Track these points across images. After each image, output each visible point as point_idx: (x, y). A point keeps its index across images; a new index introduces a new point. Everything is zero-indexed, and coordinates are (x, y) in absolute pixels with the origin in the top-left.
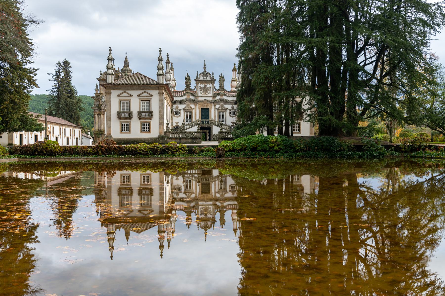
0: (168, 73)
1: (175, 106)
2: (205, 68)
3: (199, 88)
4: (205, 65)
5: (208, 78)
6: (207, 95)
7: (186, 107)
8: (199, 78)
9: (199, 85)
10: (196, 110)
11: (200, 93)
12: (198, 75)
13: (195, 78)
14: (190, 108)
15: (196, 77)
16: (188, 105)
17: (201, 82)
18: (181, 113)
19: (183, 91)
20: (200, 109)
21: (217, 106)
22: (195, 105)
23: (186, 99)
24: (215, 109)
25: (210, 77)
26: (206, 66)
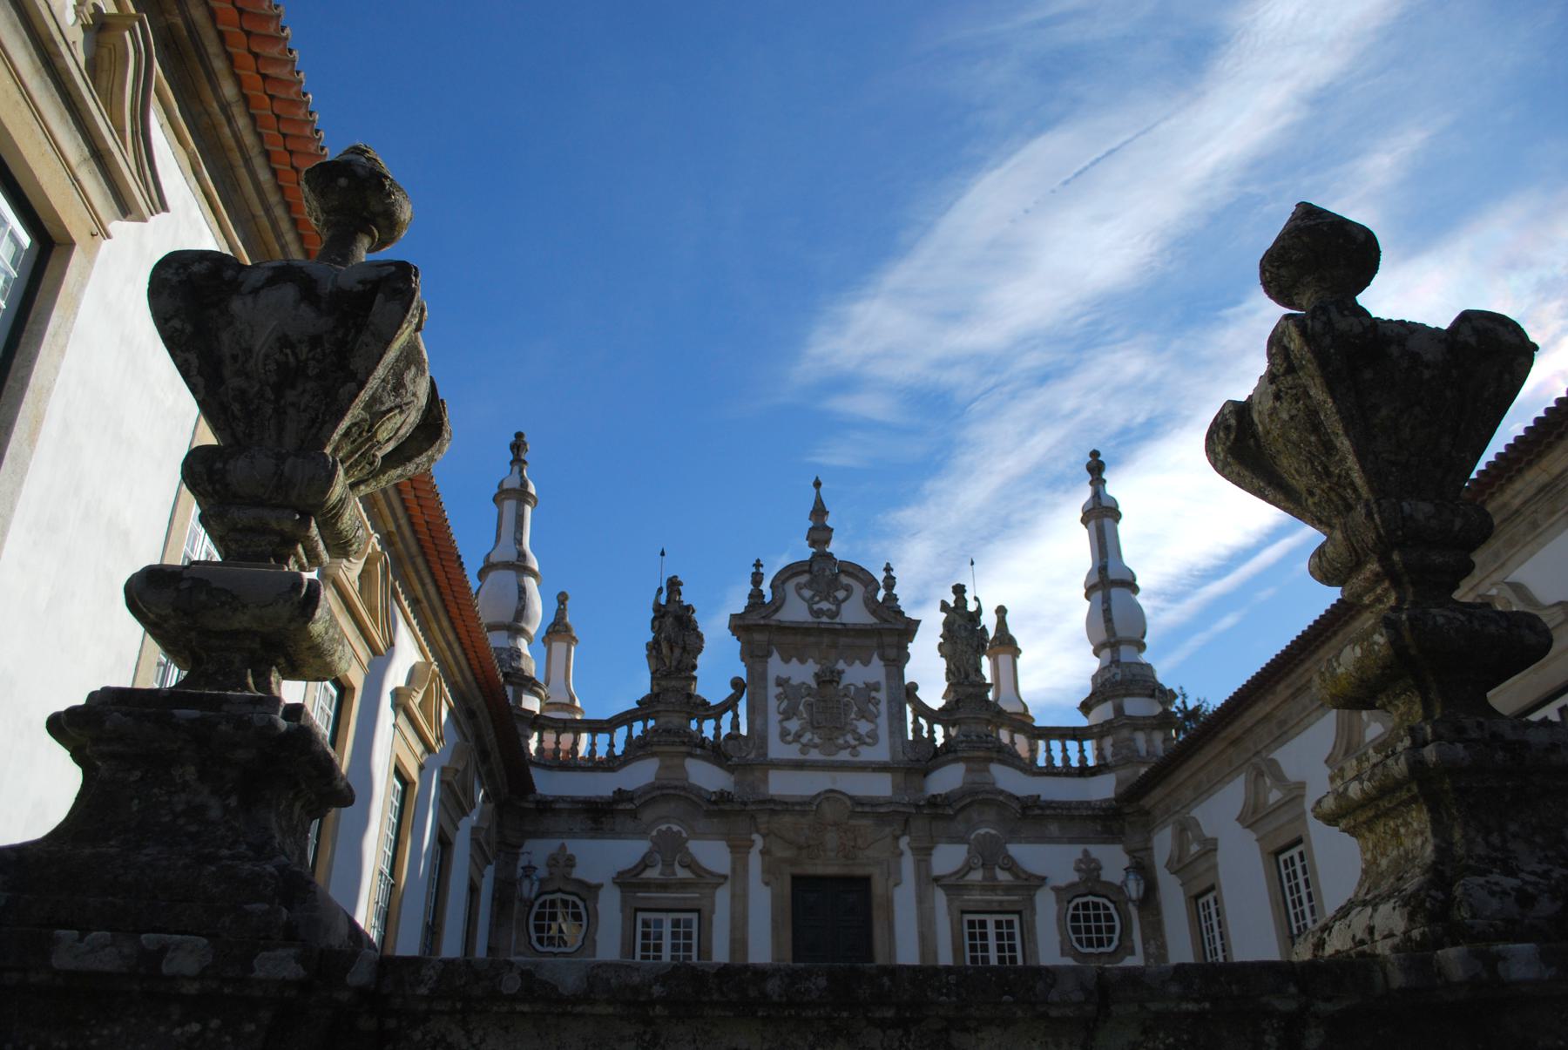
0: (507, 565)
1: (538, 851)
2: (820, 534)
3: (773, 690)
4: (819, 511)
5: (854, 613)
6: (844, 756)
7: (645, 864)
8: (778, 603)
9: (776, 666)
10: (740, 901)
11: (784, 734)
12: (765, 587)
13: (739, 604)
14: (682, 873)
15: (745, 602)
16: (671, 848)
17: (795, 640)
18: (593, 917)
19: (626, 719)
20: (786, 887)
21: (948, 858)
22: (739, 849)
23: (652, 787)
24: (928, 880)
25: (870, 601)
26: (830, 522)
